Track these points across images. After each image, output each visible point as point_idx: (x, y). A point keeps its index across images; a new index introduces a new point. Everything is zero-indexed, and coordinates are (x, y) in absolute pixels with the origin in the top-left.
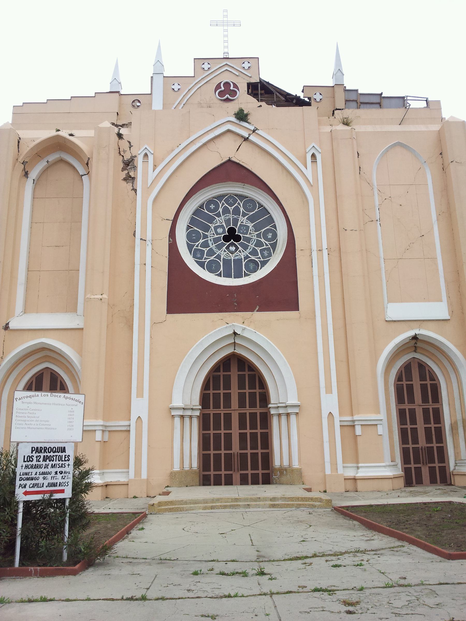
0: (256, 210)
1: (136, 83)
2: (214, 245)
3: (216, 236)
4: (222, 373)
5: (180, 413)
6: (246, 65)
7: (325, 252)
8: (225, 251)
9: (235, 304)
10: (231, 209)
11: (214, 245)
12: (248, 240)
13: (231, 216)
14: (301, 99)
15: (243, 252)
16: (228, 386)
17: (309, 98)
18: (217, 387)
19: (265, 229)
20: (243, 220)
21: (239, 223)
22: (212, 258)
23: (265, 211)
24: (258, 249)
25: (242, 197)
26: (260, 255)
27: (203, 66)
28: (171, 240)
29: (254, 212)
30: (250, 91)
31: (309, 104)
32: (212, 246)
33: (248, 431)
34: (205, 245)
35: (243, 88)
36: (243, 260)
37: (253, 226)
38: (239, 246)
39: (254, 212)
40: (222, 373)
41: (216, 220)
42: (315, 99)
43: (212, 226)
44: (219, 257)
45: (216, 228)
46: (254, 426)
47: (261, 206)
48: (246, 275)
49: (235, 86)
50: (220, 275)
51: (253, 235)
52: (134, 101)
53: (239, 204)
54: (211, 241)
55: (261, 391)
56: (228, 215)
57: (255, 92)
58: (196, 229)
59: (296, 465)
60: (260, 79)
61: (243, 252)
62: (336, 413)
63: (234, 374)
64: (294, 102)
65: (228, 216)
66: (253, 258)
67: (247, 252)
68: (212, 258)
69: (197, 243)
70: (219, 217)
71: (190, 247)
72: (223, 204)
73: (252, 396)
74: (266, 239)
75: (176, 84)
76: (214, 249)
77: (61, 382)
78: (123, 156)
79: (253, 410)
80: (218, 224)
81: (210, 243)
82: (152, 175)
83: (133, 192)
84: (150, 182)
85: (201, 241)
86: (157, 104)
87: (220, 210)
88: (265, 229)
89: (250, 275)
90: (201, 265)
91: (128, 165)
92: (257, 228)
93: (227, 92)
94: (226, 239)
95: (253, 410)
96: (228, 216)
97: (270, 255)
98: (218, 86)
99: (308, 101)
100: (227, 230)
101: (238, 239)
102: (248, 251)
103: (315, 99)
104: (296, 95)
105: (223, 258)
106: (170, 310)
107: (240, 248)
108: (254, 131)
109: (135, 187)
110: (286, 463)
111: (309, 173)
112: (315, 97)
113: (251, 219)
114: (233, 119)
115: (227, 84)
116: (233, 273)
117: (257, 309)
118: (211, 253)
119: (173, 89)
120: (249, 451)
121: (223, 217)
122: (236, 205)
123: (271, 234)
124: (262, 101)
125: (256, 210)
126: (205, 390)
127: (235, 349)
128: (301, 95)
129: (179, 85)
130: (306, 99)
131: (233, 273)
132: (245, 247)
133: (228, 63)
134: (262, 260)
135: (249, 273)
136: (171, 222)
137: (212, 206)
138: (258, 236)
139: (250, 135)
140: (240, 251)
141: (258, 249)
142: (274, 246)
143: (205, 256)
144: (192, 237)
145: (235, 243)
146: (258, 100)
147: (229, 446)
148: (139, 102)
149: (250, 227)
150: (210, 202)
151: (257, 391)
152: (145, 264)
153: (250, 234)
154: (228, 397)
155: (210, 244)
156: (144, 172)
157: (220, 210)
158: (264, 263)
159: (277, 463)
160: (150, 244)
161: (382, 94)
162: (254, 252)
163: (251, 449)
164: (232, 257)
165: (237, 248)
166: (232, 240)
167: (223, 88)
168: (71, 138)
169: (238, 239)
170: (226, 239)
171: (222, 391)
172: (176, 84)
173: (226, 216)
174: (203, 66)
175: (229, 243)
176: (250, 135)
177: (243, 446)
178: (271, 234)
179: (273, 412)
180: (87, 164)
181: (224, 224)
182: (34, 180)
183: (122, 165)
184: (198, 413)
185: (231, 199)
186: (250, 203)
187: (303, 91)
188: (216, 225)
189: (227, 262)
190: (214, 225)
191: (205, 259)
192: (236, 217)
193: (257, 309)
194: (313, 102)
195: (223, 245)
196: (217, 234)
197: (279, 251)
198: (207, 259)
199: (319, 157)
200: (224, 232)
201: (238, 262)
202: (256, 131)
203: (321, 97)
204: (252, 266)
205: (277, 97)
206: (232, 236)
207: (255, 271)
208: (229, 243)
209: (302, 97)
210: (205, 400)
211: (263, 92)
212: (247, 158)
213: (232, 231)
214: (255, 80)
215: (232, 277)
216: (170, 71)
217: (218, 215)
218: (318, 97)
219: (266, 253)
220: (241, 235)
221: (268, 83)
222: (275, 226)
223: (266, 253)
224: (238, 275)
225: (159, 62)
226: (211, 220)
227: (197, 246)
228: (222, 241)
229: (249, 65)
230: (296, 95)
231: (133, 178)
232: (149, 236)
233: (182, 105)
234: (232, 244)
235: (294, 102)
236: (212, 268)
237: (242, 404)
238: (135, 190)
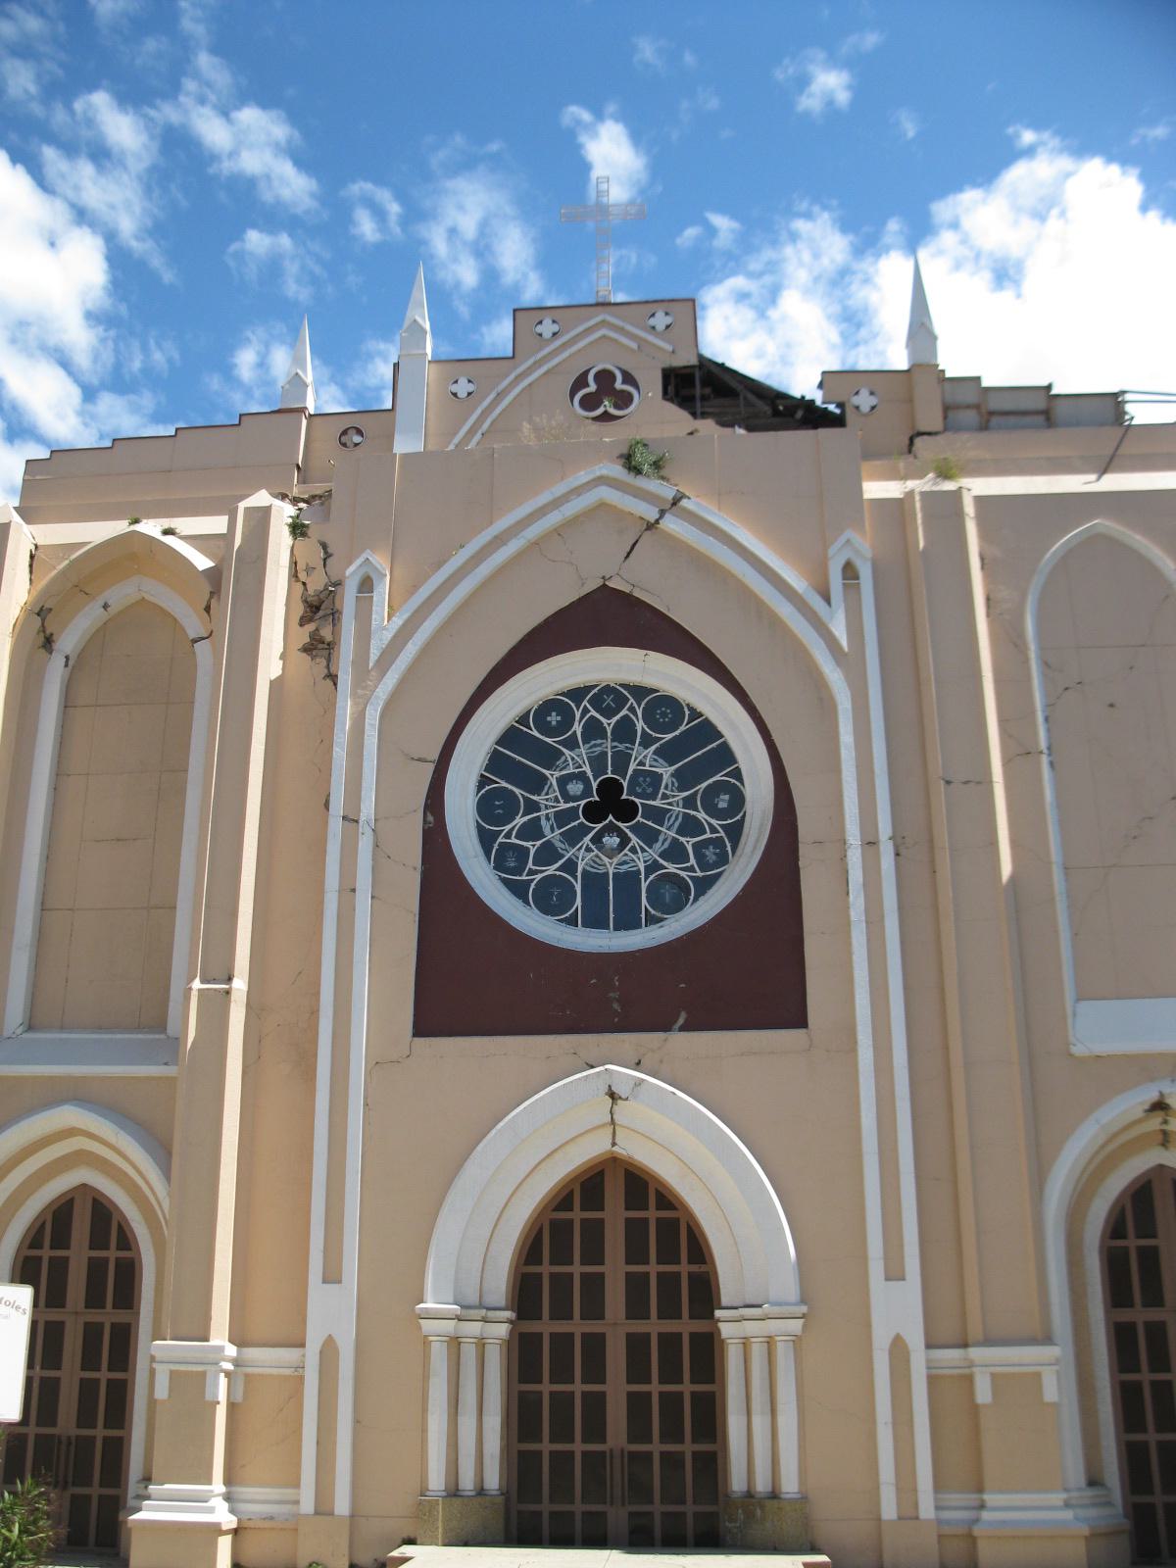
0: (683, 728)
2: (557, 832)
3: (563, 806)
4: (577, 1215)
5: (449, 1326)
6: (660, 321)
7: (887, 850)
8: (588, 850)
9: (616, 1006)
10: (609, 724)
11: (557, 832)
12: (659, 815)
13: (608, 746)
14: (818, 408)
15: (643, 850)
16: (594, 1252)
17: (840, 405)
18: (562, 1255)
19: (710, 781)
20: (642, 757)
21: (632, 766)
22: (551, 870)
23: (706, 731)
24: (688, 842)
25: (639, 692)
26: (693, 861)
27: (539, 329)
28: (430, 818)
29: (677, 733)
30: (671, 389)
31: (838, 421)
32: (552, 835)
33: (655, 1388)
34: (532, 831)
35: (651, 385)
36: (643, 876)
37: (672, 775)
38: (630, 834)
39: (677, 733)
40: (577, 1215)
41: (563, 758)
42: (857, 408)
43: (553, 776)
44: (570, 866)
45: (563, 781)
46: (671, 1373)
47: (695, 714)
48: (652, 920)
49: (628, 378)
50: (572, 921)
51: (672, 800)
52: (345, 433)
53: (632, 709)
54: (547, 818)
55: (695, 1268)
56: (599, 741)
57: (685, 392)
58: (504, 784)
59: (790, 1486)
60: (701, 357)
61: (643, 850)
62: (915, 1339)
63: (615, 1215)
64: (799, 414)
65: (600, 745)
66: (672, 868)
67: (653, 853)
68: (551, 870)
69: (507, 828)
70: (571, 749)
71: (486, 839)
72: (586, 711)
73: (669, 1282)
74: (713, 811)
75: (463, 381)
76: (558, 844)
77: (120, 1227)
78: (304, 584)
79: (670, 1326)
80: (571, 770)
81: (545, 825)
83: (329, 682)
84: (374, 654)
85: (520, 820)
87: (578, 728)
88: (710, 781)
89: (662, 920)
90: (518, 890)
91: (318, 608)
92: (684, 780)
93: (602, 393)
94: (593, 813)
95: (670, 1326)
96: (600, 745)
97: (723, 860)
98: (581, 382)
99: (838, 411)
100: (595, 786)
101: (627, 811)
102: (658, 847)
103: (857, 408)
104: (803, 397)
105: (585, 872)
106: (424, 1026)
107: (635, 840)
108: (675, 502)
109: (333, 670)
110: (762, 1485)
112: (856, 400)
113: (668, 753)
114: (617, 471)
115: (605, 377)
116: (612, 916)
117: (681, 1021)
118: (548, 854)
119: (455, 395)
120: (656, 1447)
121: (583, 750)
122: (624, 712)
123: (727, 797)
124: (704, 415)
125: (683, 728)
126: (527, 1263)
127: (614, 1144)
128: (818, 397)
129: (469, 381)
130: (832, 407)
131: (612, 916)
132: (650, 837)
133: (609, 318)
134: (699, 874)
135: (659, 914)
136: (431, 767)
137: (554, 718)
138: (689, 802)
139: (662, 513)
140: (633, 850)
141: (688, 842)
142: (735, 832)
143: (530, 865)
144: (492, 808)
145: (620, 824)
146: (694, 415)
147: (596, 1429)
148: (359, 432)
149: (666, 778)
150: (548, 706)
151: (684, 1268)
152: (354, 890)
153: (665, 797)
154: (594, 1286)
155: (547, 830)
157: (578, 728)
158: (704, 885)
159: (737, 1483)
160: (369, 834)
161: (1049, 387)
162: (676, 853)
163: (663, 1439)
164: (610, 866)
165: (625, 840)
166: (611, 817)
167: (592, 387)
168: (169, 540)
169: (627, 811)
170: (593, 813)
171: (577, 1269)
172: (463, 381)
173: (595, 746)
174: (539, 329)
175: (601, 825)
176: (662, 513)
177: (638, 1429)
178: (727, 797)
179: (726, 1330)
180: (208, 609)
181: (587, 769)
182: (67, 658)
183: (299, 609)
184: (502, 1330)
185: (608, 697)
186: (664, 708)
187: (821, 386)
188: (564, 772)
189: (594, 882)
190: (557, 774)
191: (532, 872)
192: (621, 747)
193: (681, 1021)
194: (850, 416)
195: (583, 830)
196: (567, 798)
197: (748, 849)
198: (537, 872)
200: (587, 792)
201: (628, 881)
202: (684, 503)
203: (873, 401)
204: (668, 893)
205: (748, 404)
206: (610, 804)
207: (677, 906)
208: (601, 825)
209: (819, 402)
210: (525, 1295)
211: (708, 391)
213: (610, 788)
214: (684, 359)
215: (608, 928)
217: (572, 744)
218: (864, 401)
219: (710, 854)
220: (637, 800)
221: (722, 366)
222: (737, 774)
223: (710, 854)
224: (628, 921)
226: (550, 757)
227: (508, 835)
228: (582, 819)
229: (669, 320)
230: (803, 397)
231: (329, 644)
233: (478, 436)
234: (611, 829)
235: (799, 414)
236: (550, 899)
237: (636, 1307)
238: (333, 678)
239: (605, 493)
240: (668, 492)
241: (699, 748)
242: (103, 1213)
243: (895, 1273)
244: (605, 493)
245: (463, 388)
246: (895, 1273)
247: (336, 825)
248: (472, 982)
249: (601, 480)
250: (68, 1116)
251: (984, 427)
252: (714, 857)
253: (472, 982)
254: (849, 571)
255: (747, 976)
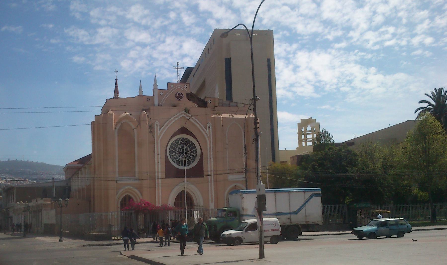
1: (148, 92)
12: (188, 153)
23: (193, 144)
35: (185, 95)
43: (177, 149)
82: (159, 132)
86: (156, 103)
92: (191, 149)
98: (176, 94)
111: (208, 132)
132: (187, 156)
142: (196, 156)
150: (176, 140)
156: (157, 131)
186: (189, 141)
199: (211, 127)
212: (188, 126)
216: (159, 87)
218: (210, 101)
225: (155, 84)
226: (177, 146)
232: (159, 153)
239: (183, 115)
240: (190, 116)
241: (192, 146)
242: (130, 198)
243: (212, 202)
244: (183, 115)
245: (162, 94)
246: (212, 202)
247: (156, 155)
248: (172, 173)
249: (183, 113)
250: (129, 187)
251: (222, 106)
252: (194, 158)
253: (172, 173)
254: (209, 127)
255: (198, 172)
